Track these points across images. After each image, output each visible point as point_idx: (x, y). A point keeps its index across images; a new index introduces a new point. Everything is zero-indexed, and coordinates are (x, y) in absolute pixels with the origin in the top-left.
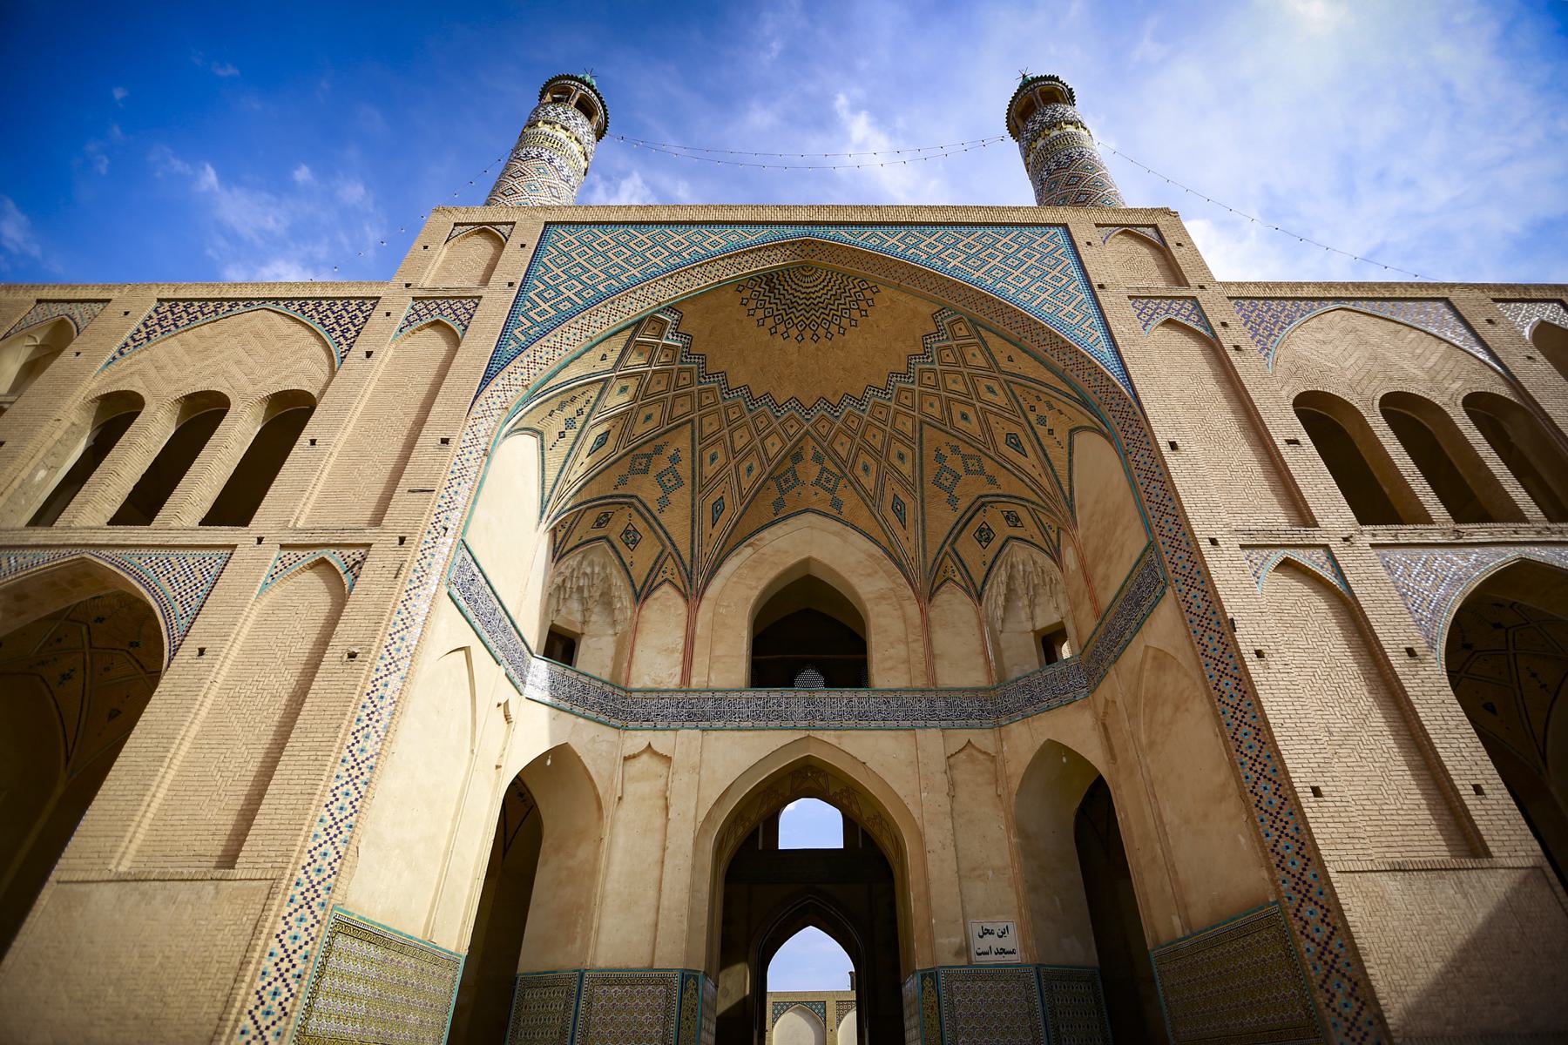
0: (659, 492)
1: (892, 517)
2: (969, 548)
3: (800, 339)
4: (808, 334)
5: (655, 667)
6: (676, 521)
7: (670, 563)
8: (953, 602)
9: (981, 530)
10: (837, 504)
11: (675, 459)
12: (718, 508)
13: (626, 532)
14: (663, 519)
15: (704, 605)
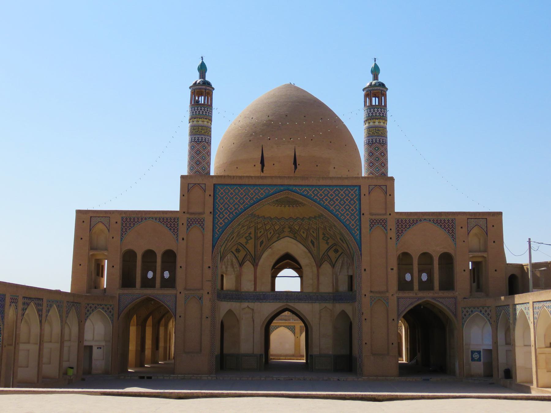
0: (245, 240)
1: (311, 244)
2: (332, 254)
3: (285, 206)
4: (287, 206)
5: (247, 286)
6: (250, 246)
7: (249, 256)
8: (326, 266)
9: (335, 250)
10: (296, 238)
11: (250, 234)
12: (262, 243)
13: (237, 249)
14: (246, 246)
15: (259, 268)
